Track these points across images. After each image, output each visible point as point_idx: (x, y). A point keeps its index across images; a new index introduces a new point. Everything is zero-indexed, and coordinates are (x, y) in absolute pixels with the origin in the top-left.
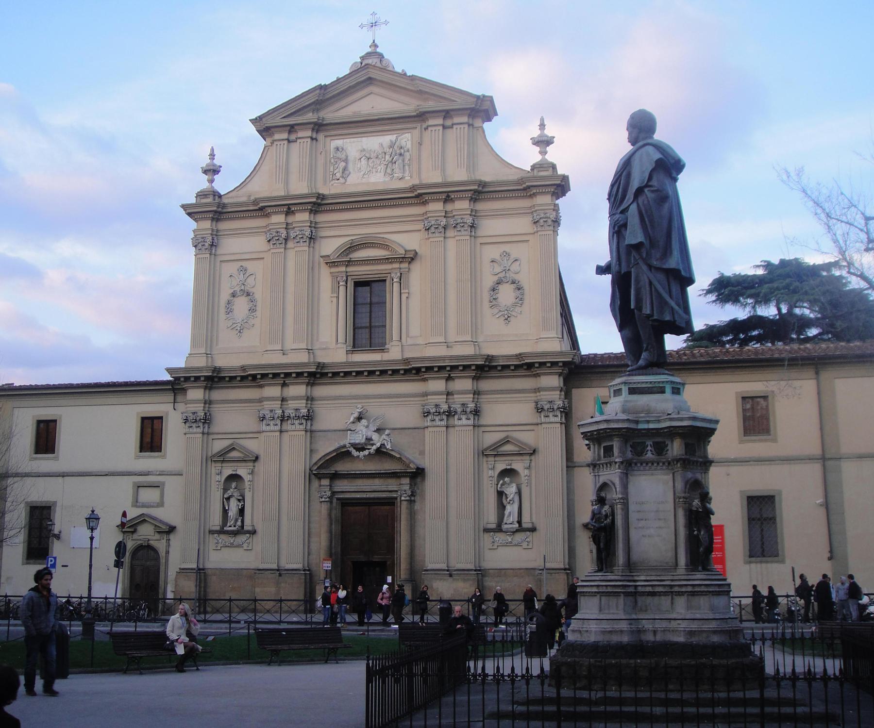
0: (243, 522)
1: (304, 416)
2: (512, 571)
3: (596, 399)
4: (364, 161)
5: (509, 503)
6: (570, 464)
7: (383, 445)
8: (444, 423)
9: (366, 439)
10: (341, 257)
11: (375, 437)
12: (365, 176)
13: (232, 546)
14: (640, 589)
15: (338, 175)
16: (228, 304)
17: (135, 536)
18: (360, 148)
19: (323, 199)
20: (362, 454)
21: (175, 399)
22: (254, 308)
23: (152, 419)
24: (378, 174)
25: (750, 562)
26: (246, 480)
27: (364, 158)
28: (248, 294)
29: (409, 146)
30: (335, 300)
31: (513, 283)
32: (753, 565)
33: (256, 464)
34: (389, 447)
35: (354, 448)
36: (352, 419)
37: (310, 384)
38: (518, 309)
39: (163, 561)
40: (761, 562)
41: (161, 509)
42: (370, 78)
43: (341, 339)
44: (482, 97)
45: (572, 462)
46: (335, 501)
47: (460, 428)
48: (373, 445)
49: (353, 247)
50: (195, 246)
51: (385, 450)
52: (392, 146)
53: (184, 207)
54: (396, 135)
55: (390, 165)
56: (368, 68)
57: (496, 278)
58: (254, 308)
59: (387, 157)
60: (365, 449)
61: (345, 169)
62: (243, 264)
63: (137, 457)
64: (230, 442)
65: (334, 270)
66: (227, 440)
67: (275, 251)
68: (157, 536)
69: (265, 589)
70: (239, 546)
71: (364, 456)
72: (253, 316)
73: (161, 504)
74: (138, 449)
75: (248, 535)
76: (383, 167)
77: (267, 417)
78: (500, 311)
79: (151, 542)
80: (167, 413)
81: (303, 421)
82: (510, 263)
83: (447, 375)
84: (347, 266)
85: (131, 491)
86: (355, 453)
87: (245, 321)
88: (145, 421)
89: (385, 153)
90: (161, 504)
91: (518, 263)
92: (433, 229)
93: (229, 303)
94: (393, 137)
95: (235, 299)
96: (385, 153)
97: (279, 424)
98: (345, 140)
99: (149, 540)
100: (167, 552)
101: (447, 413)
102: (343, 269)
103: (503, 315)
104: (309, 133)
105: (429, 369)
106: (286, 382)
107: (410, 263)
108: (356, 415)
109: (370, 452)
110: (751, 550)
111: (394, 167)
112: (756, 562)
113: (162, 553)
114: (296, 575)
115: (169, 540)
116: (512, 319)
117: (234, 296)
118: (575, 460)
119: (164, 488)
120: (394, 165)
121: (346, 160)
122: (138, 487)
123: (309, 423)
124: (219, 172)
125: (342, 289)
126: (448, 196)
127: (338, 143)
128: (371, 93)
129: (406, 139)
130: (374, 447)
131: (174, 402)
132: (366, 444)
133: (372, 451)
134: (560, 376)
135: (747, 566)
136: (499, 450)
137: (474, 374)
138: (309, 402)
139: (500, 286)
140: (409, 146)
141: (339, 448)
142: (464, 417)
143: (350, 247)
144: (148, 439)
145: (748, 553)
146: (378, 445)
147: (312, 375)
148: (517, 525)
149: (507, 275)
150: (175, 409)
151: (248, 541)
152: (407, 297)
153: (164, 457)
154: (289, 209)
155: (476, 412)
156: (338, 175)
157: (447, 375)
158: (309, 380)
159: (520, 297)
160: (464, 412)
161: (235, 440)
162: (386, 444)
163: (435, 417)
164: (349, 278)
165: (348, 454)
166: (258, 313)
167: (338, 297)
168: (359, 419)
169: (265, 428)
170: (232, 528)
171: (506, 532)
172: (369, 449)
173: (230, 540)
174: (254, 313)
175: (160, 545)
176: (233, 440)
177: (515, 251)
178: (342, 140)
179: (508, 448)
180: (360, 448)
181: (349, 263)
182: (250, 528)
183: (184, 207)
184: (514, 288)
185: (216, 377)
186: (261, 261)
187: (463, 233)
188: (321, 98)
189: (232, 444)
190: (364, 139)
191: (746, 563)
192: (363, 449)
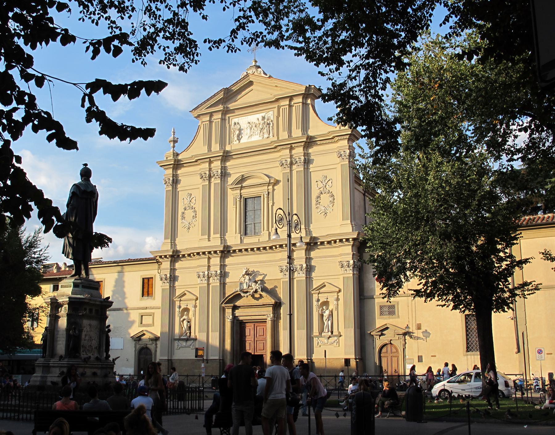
0: (190, 333)
4: (249, 129)
6: (362, 297)
13: (185, 347)
14: (51, 365)
15: (236, 138)
17: (140, 342)
25: (467, 355)
29: (272, 118)
32: (469, 357)
39: (153, 356)
40: (474, 355)
45: (364, 296)
46: (235, 321)
52: (264, 118)
61: (238, 136)
63: (141, 300)
70: (189, 347)
74: (141, 296)
75: (193, 341)
79: (148, 346)
82: (326, 181)
90: (153, 324)
93: (183, 213)
94: (263, 114)
99: (147, 344)
100: (156, 351)
110: (467, 348)
111: (264, 132)
112: (471, 355)
113: (153, 352)
115: (157, 344)
117: (185, 210)
118: (366, 294)
119: (154, 316)
121: (240, 130)
125: (238, 202)
126: (292, 146)
127: (236, 120)
135: (466, 357)
139: (321, 195)
145: (466, 350)
148: (330, 334)
165: (239, 294)
167: (236, 208)
173: (184, 344)
175: (152, 347)
182: (194, 337)
185: (175, 255)
191: (464, 356)
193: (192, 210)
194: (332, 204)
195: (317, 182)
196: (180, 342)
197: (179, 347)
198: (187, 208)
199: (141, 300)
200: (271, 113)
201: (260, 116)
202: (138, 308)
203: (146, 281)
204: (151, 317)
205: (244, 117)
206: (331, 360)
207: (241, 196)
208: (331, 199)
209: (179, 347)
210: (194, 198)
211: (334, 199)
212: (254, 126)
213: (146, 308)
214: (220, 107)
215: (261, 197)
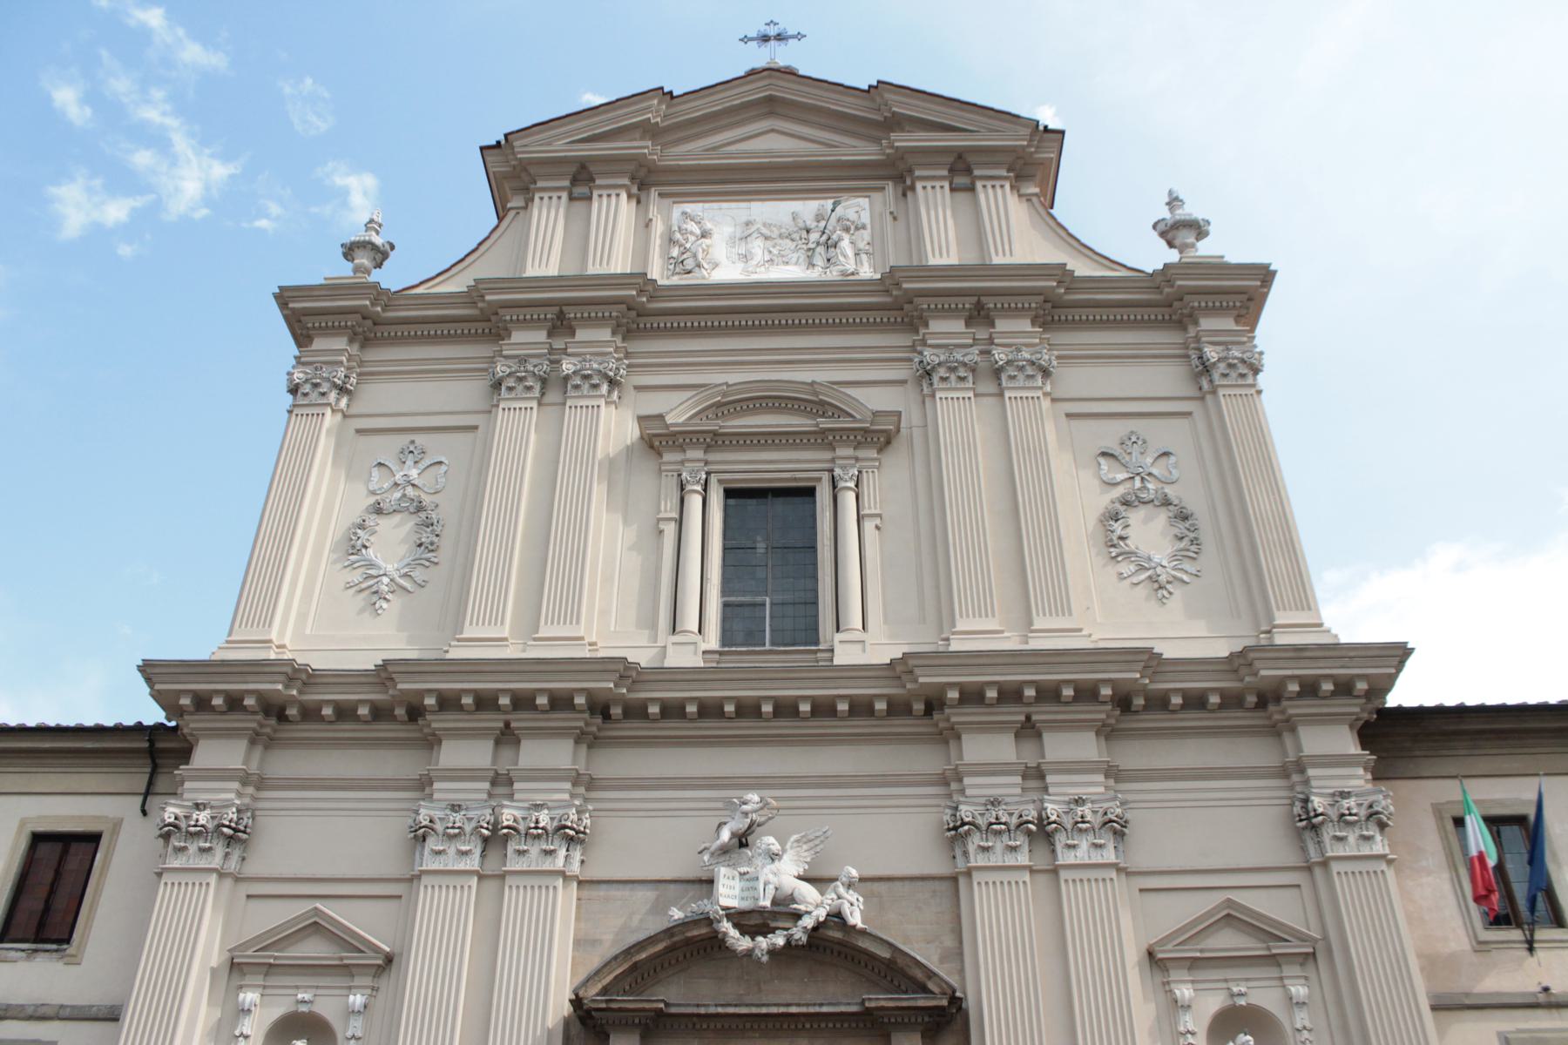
1: (565, 827)
3: (1438, 810)
7: (837, 917)
8: (1023, 858)
9: (774, 902)
10: (693, 421)
11: (808, 892)
12: (758, 270)
16: (362, 526)
18: (744, 219)
19: (651, 298)
20: (763, 942)
21: (150, 783)
22: (436, 539)
23: (66, 840)
26: (340, 1036)
27: (755, 235)
28: (420, 508)
30: (670, 530)
31: (1166, 503)
33: (383, 982)
34: (855, 919)
35: (736, 926)
36: (725, 835)
37: (588, 740)
38: (1187, 566)
44: (1041, 128)
47: (1077, 874)
48: (797, 916)
49: (724, 407)
50: (294, 390)
51: (838, 935)
53: (284, 297)
54: (832, 201)
55: (821, 249)
56: (770, 77)
57: (1119, 491)
58: (436, 539)
59: (814, 236)
60: (773, 931)
62: (421, 439)
64: (303, 907)
65: (667, 457)
66: (287, 903)
71: (773, 952)
72: (428, 560)
76: (802, 255)
77: (439, 827)
78: (1143, 568)
80: (117, 825)
81: (557, 843)
84: (708, 448)
86: (740, 942)
87: (403, 571)
88: (44, 849)
89: (808, 232)
91: (1172, 459)
92: (942, 372)
94: (829, 204)
96: (808, 232)
97: (478, 852)
98: (707, 205)
101: (1031, 826)
102: (699, 454)
104: (626, 181)
105: (972, 696)
107: (880, 451)
108: (740, 824)
109: (788, 943)
123: (577, 855)
124: (385, 256)
125: (695, 502)
128: (773, 131)
129: (858, 208)
130: (808, 922)
131: (147, 794)
132: (774, 915)
133: (799, 934)
134: (1351, 727)
137: (1103, 716)
138: (582, 790)
140: (865, 218)
141: (685, 925)
142: (1084, 844)
143: (719, 405)
144: (32, 903)
146: (821, 914)
147: (600, 708)
149: (1150, 486)
150: (144, 813)
152: (877, 528)
153: (75, 961)
155: (1117, 829)
156: (690, 264)
157: (1022, 718)
158: (587, 724)
159: (1192, 535)
160: (1080, 826)
161: (319, 905)
162: (846, 909)
163: (991, 837)
164: (713, 479)
165: (713, 945)
166: (443, 555)
167: (680, 522)
168: (742, 841)
169: (431, 864)
172: (787, 929)
174: (430, 555)
177: (1161, 434)
178: (701, 205)
179: (1228, 941)
180: (753, 921)
181: (715, 441)
183: (284, 297)
184: (1171, 514)
185: (292, 701)
186: (469, 436)
187: (1021, 382)
188: (659, 119)
190: (754, 205)
192: (765, 930)
193: (423, 515)
194: (1193, 548)
195: (1104, 454)
200: (864, 202)
201: (808, 209)
203: (47, 851)
205: (733, 205)
207: (708, 473)
208: (1181, 527)
210: (444, 468)
212: (775, 233)
215: (810, 492)
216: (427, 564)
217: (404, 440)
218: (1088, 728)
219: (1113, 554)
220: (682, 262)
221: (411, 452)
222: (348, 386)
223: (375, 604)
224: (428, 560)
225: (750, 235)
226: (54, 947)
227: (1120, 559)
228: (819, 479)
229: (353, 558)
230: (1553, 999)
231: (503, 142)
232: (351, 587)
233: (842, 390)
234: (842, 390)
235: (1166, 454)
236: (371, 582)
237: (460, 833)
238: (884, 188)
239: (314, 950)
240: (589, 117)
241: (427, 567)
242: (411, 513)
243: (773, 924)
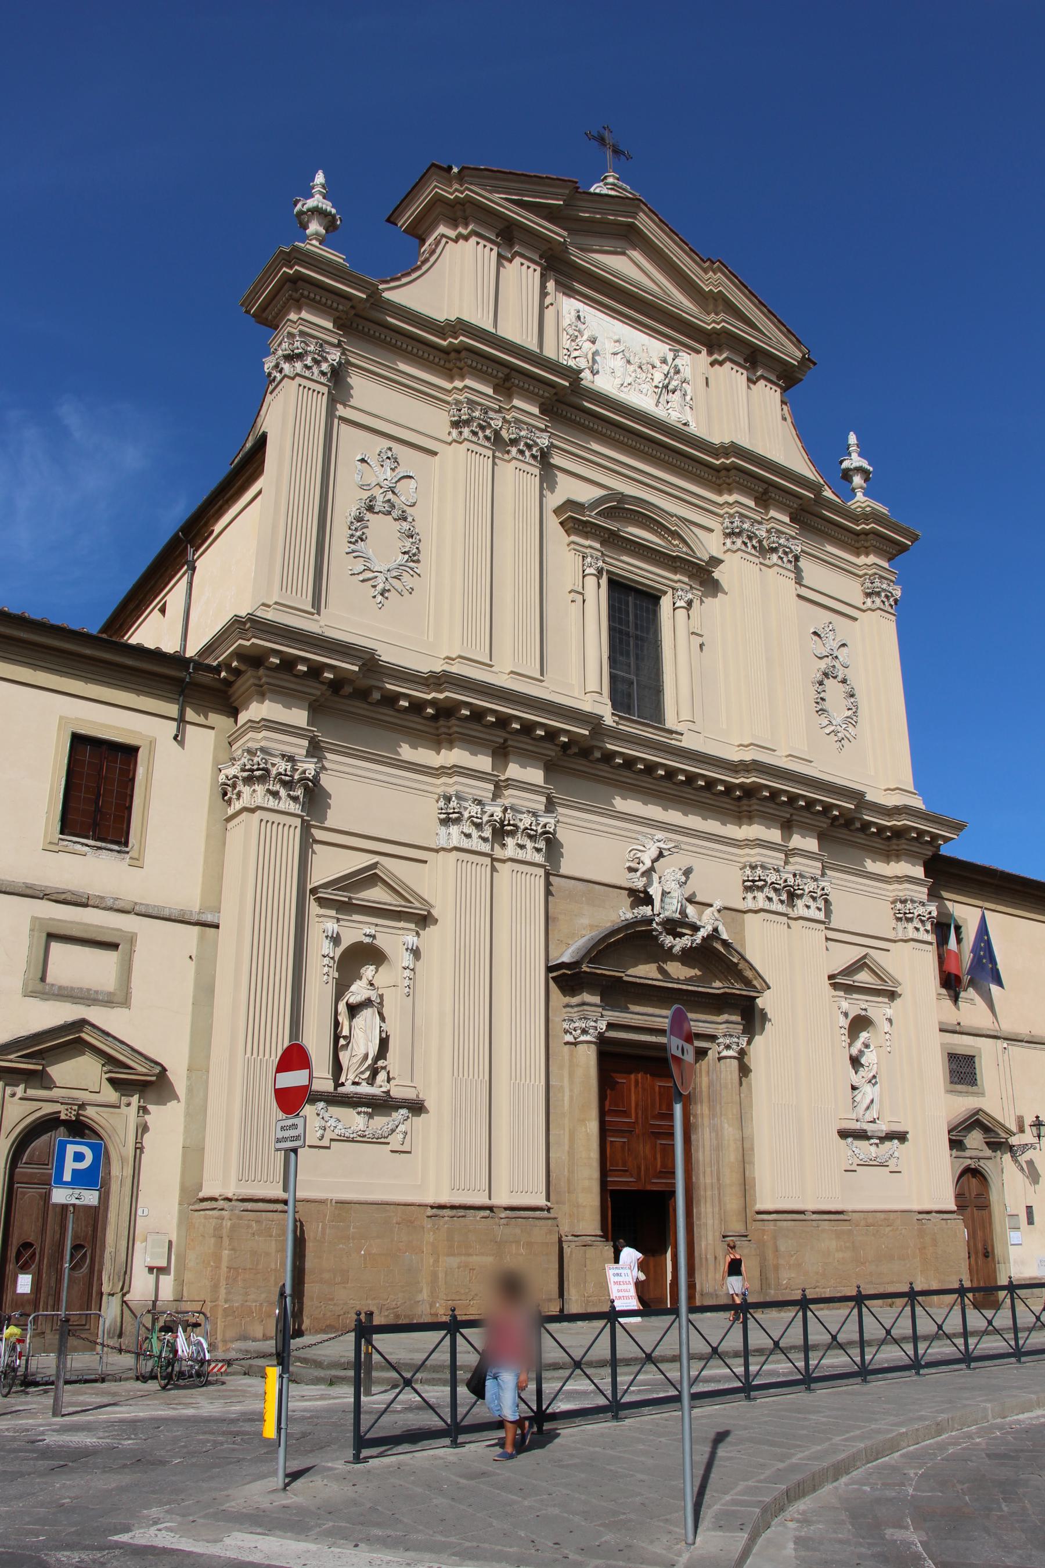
2: (882, 1216)
5: (870, 1082)
13: (362, 1139)
24: (642, 396)
27: (620, 356)
31: (844, 681)
41: (118, 1012)
42: (632, 227)
43: (593, 685)
56: (638, 206)
62: (397, 448)
63: (50, 848)
64: (367, 860)
67: (473, 447)
68: (110, 1095)
69: (471, 1259)
70: (379, 1140)
72: (412, 569)
73: (119, 998)
79: (90, 1112)
80: (152, 743)
83: (788, 816)
85: (26, 941)
86: (668, 940)
90: (119, 998)
95: (368, 516)
99: (82, 1106)
103: (835, 732)
106: (510, 743)
114: (542, 1222)
116: (845, 742)
119: (131, 952)
120: (670, 394)
122: (52, 937)
130: (702, 933)
136: (856, 978)
151: (402, 1128)
152: (701, 646)
154: (507, 378)
170: (365, 1089)
171: (868, 1138)
173: (355, 1120)
176: (376, 858)
189: (375, 866)
196: (336, 1111)
197: (329, 1135)
198: (379, 505)
199: (50, 848)
202: (28, 886)
204: (111, 958)
206: (892, 1216)
209: (329, 1135)
211: (857, 707)
213: (81, 902)
214: (556, 233)
216: (412, 573)
217: (387, 443)
218: (812, 830)
219: (817, 709)
220: (575, 358)
221: (388, 458)
222: (296, 351)
223: (374, 597)
224: (412, 569)
225: (617, 354)
226: (116, 847)
227: (820, 713)
228: (665, 593)
229: (353, 547)
230: (962, 1030)
231: (455, 170)
232: (354, 574)
233: (691, 527)
234: (691, 527)
235: (844, 645)
236: (370, 575)
237: (459, 817)
238: (700, 352)
239: (376, 895)
240: (522, 182)
241: (412, 576)
242: (395, 520)
243: (679, 930)
